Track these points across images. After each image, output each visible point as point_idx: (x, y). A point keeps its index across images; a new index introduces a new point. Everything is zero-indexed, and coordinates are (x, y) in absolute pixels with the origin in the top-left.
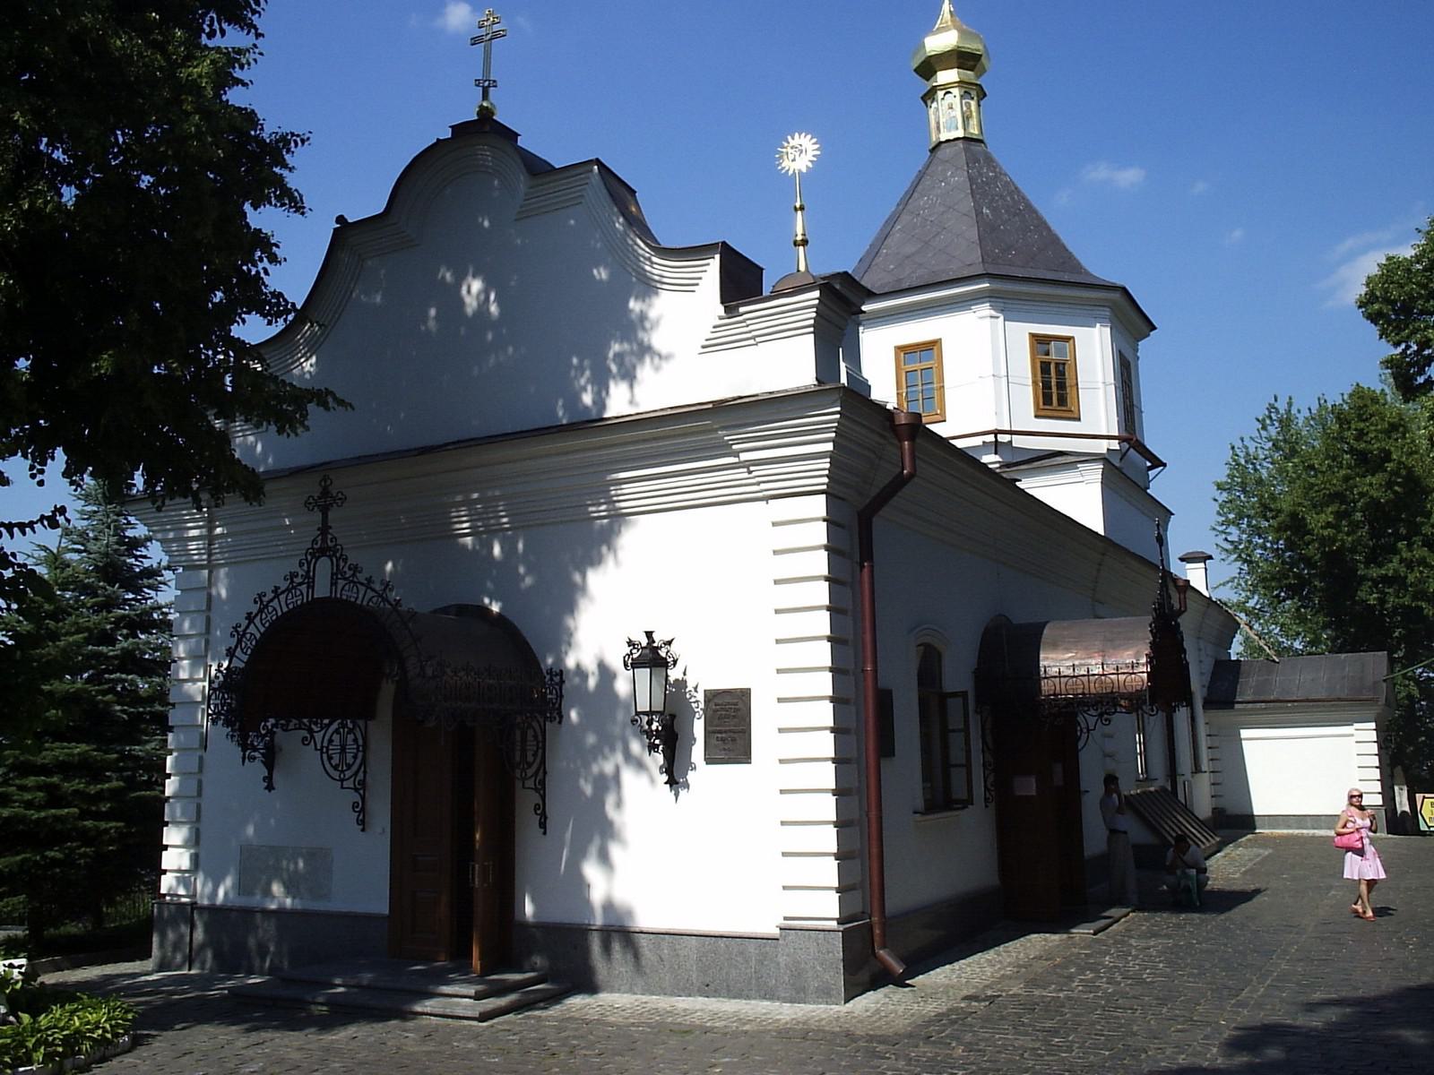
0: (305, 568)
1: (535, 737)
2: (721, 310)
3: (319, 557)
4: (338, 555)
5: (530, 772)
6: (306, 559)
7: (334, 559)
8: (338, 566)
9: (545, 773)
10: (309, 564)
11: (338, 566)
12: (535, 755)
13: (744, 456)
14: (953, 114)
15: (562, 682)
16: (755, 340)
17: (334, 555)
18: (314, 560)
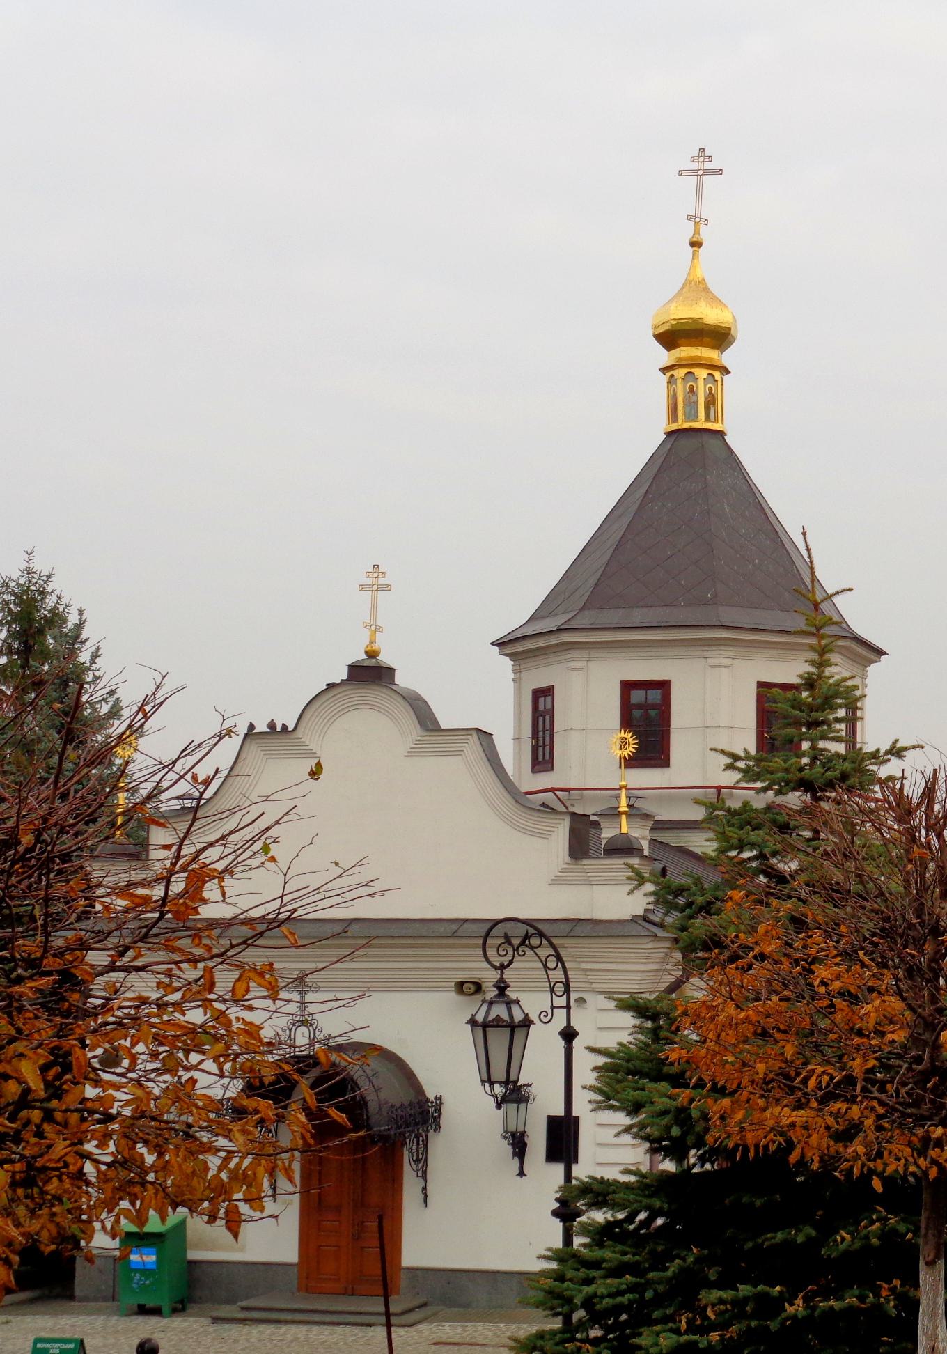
0: (288, 1032)
1: (423, 1141)
2: (568, 859)
3: (299, 1026)
4: (314, 1026)
5: (420, 1165)
6: (288, 1027)
7: (311, 1028)
8: (314, 1035)
9: (427, 1165)
10: (290, 1031)
11: (314, 1035)
12: (422, 1154)
13: (584, 966)
14: (693, 399)
15: (441, 1103)
16: (590, 883)
17: (311, 1025)
18: (294, 1028)
